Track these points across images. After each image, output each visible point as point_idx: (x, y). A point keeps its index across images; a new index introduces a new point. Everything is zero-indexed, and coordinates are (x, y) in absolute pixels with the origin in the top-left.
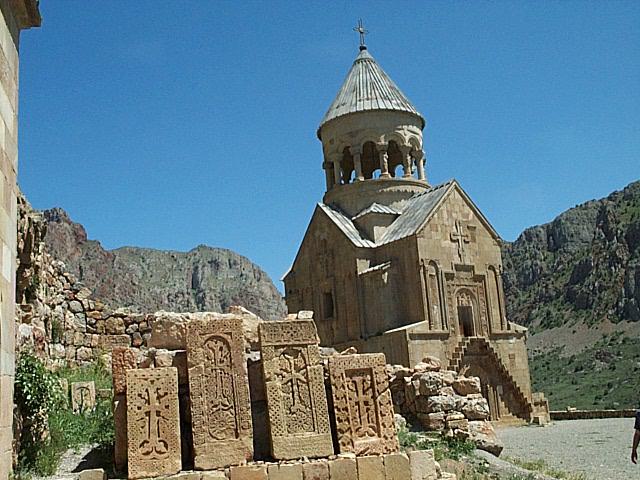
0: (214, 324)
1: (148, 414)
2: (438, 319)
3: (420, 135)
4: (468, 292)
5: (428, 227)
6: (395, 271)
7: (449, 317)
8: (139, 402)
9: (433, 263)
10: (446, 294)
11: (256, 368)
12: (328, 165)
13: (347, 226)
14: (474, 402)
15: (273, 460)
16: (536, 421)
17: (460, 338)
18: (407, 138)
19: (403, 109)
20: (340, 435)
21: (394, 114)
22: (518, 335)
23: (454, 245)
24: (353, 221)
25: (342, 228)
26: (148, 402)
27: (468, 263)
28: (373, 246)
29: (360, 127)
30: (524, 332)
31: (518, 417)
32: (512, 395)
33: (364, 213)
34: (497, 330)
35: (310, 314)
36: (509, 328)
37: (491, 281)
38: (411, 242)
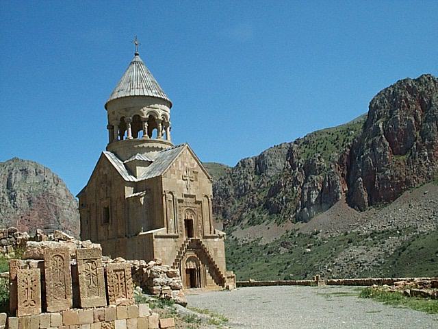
0: (56, 250)
1: (27, 289)
2: (172, 227)
4: (191, 210)
6: (148, 197)
7: (179, 226)
8: (23, 284)
9: (171, 193)
11: (74, 268)
12: (110, 127)
13: (120, 167)
14: (175, 281)
15: (81, 308)
16: (228, 288)
17: (185, 238)
18: (160, 114)
19: (159, 96)
20: (110, 297)
25: (117, 168)
26: (27, 283)
27: (192, 194)
28: (136, 180)
31: (217, 284)
33: (131, 160)
34: (207, 234)
36: (215, 233)
37: (205, 204)
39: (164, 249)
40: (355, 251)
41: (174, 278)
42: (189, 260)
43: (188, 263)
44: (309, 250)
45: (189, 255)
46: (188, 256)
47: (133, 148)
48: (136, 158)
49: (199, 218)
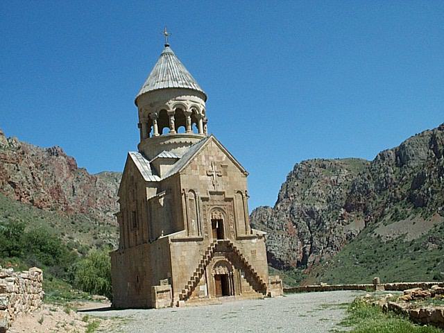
2: (195, 228)
3: (201, 104)
4: (220, 209)
9: (191, 190)
10: (202, 212)
12: (140, 125)
16: (269, 296)
18: (189, 106)
19: (186, 87)
21: (179, 90)
28: (159, 179)
29: (157, 100)
30: (264, 235)
31: (256, 291)
32: (252, 278)
36: (252, 233)
38: (176, 177)
39: (185, 254)
42: (218, 265)
43: (217, 269)
45: (216, 259)
46: (217, 261)
47: (160, 145)
48: (160, 156)
49: (231, 218)
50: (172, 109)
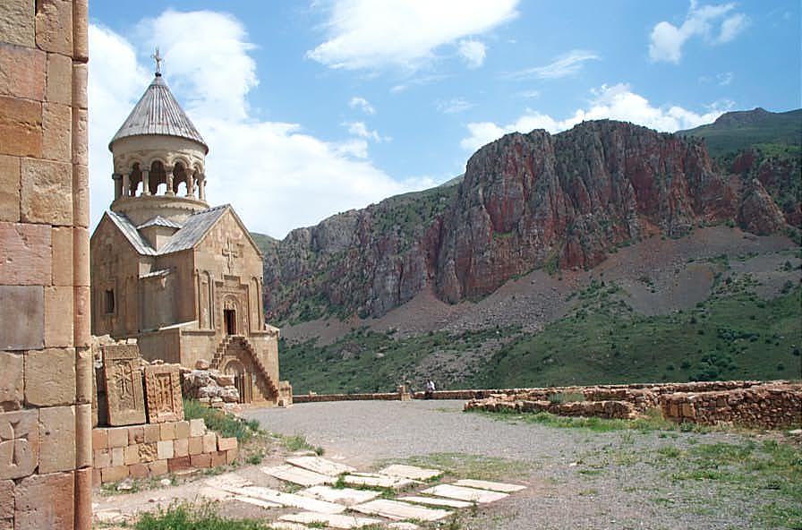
2: (207, 320)
4: (233, 298)
5: (204, 243)
7: (216, 317)
9: (206, 272)
12: (117, 177)
13: (132, 235)
14: (229, 391)
15: (110, 426)
16: (281, 404)
17: (224, 336)
18: (192, 162)
19: (191, 137)
21: (182, 140)
22: (272, 334)
23: (225, 259)
24: (137, 230)
25: (128, 236)
27: (235, 274)
28: (155, 254)
29: (151, 148)
30: (277, 332)
33: (147, 225)
35: (135, 340)
36: (265, 329)
40: (443, 356)
41: (227, 387)
44: (381, 355)
45: (229, 359)
46: (228, 361)
47: (151, 205)
48: (156, 222)
49: (244, 309)
50: (171, 163)
